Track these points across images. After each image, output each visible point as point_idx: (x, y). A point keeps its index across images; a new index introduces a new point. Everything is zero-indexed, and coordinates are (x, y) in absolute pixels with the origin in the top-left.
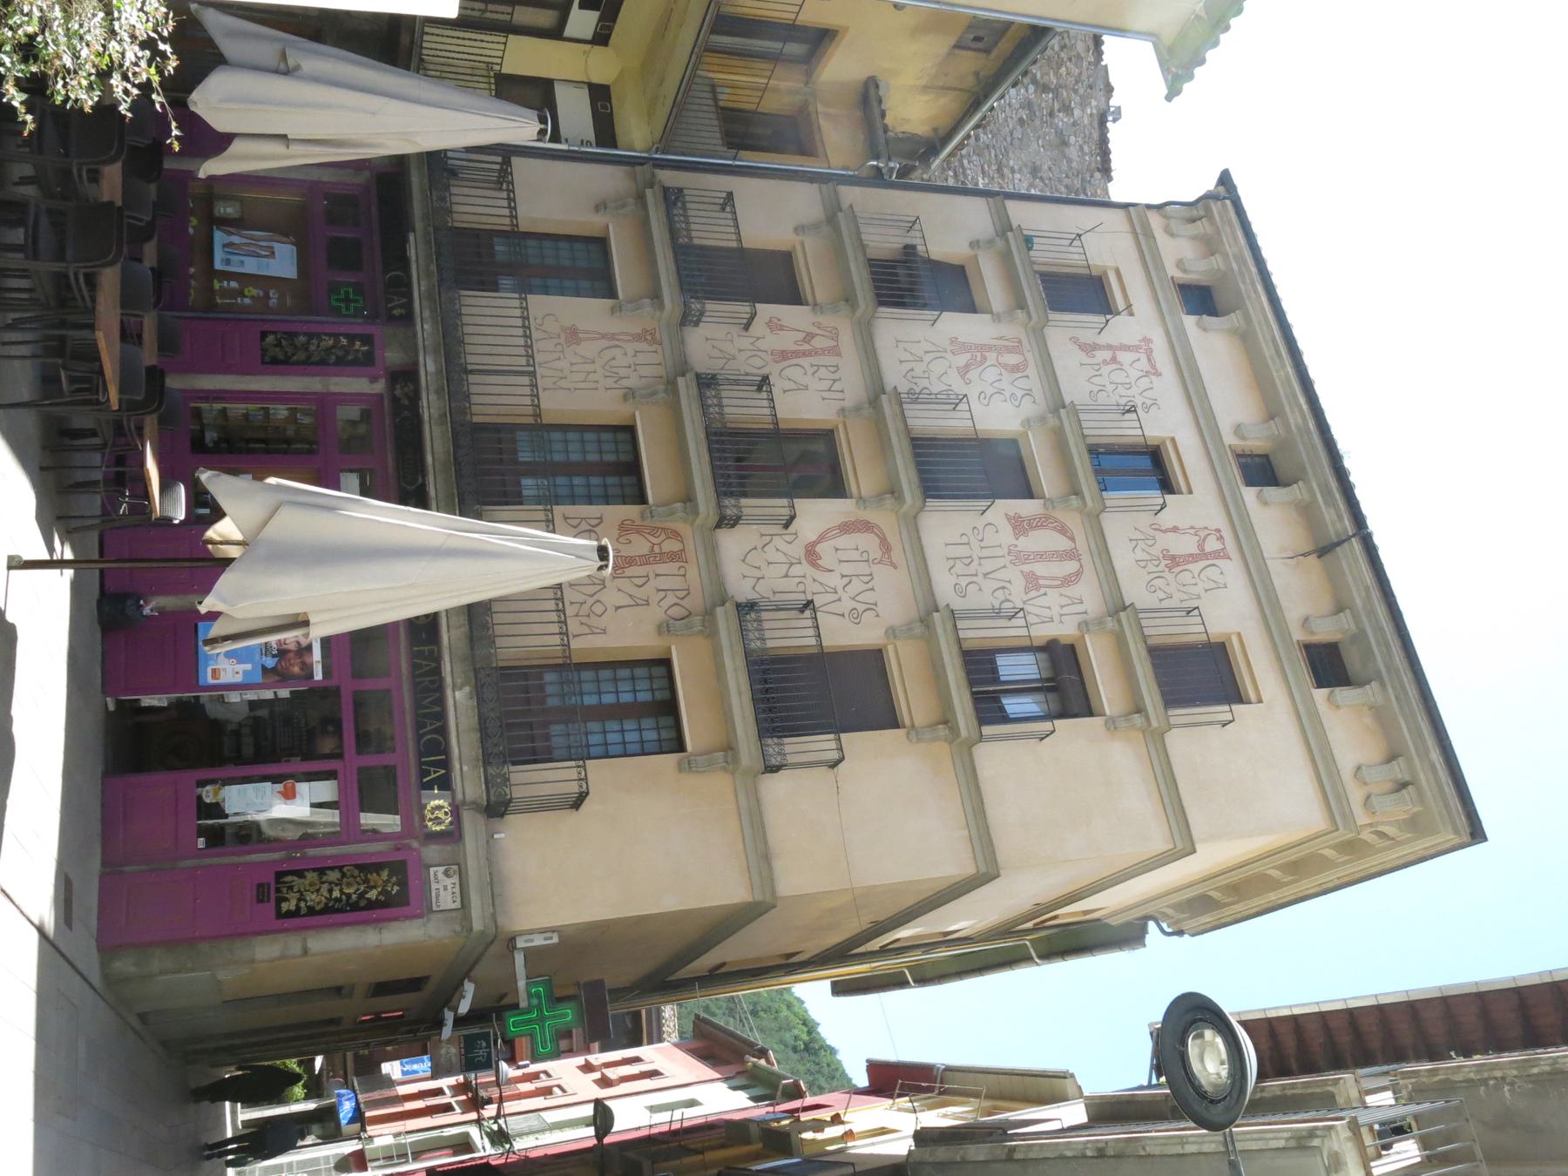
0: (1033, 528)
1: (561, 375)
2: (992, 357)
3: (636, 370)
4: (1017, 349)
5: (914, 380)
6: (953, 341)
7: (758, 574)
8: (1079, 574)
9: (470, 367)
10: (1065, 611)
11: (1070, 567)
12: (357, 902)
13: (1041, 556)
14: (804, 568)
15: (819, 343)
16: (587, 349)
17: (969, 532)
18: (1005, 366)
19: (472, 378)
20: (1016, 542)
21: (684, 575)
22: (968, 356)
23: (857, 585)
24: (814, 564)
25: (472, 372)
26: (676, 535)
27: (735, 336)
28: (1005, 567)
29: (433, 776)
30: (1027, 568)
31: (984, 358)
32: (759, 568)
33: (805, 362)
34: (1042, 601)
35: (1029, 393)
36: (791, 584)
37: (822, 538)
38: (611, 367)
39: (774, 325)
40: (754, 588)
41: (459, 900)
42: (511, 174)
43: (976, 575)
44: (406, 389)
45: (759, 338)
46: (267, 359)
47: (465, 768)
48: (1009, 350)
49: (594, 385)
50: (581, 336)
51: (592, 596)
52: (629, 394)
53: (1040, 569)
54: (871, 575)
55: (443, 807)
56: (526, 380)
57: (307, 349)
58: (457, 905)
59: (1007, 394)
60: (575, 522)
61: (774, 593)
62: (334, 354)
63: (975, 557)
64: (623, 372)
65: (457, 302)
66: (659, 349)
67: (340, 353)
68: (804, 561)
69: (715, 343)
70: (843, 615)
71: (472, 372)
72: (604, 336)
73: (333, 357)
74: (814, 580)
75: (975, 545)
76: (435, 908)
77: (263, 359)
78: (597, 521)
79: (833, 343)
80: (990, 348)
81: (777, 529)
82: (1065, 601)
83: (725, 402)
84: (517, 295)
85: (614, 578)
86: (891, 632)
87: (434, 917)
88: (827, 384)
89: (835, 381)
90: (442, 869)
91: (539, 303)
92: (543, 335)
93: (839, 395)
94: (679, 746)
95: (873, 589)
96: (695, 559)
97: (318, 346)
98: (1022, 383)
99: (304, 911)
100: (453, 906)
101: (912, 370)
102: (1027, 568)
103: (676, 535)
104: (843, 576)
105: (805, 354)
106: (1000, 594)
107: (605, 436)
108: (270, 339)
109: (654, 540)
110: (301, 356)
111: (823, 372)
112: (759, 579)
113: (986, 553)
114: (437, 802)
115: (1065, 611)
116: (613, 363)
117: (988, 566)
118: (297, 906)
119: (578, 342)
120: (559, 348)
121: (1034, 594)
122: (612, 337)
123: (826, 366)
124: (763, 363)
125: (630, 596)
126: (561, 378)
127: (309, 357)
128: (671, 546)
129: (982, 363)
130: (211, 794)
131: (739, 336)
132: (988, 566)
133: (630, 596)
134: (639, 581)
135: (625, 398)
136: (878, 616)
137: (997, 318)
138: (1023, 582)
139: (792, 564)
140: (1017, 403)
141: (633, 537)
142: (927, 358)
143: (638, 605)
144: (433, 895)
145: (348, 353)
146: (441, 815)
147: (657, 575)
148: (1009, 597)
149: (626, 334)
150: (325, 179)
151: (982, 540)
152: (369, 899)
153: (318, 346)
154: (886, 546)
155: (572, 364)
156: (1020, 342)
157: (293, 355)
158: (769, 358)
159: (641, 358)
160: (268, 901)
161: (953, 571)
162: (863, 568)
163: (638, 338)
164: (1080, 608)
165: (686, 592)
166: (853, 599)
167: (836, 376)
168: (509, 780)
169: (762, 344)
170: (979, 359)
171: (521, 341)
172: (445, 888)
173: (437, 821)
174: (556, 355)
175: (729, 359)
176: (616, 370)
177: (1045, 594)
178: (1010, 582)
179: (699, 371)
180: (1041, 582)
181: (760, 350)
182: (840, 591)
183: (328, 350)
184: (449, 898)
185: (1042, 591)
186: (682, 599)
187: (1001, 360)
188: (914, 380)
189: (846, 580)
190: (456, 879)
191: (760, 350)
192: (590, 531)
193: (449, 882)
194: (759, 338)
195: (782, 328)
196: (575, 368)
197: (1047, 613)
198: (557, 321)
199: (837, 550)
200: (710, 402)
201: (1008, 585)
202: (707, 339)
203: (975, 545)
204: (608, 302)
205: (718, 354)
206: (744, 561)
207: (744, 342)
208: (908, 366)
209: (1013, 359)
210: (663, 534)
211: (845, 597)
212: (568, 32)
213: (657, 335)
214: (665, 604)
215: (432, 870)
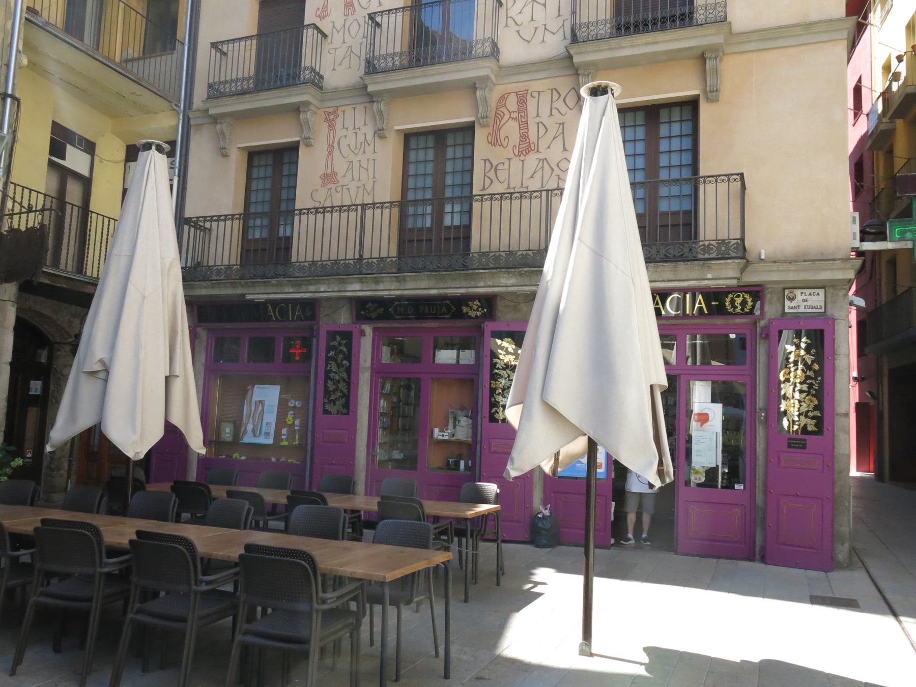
1: (361, 190)
3: (359, 128)
7: (541, 30)
9: (357, 256)
12: (815, 371)
16: (340, 167)
19: (366, 255)
21: (539, 93)
25: (361, 255)
26: (503, 98)
29: (703, 305)
32: (536, 29)
38: (356, 148)
39: (324, 12)
40: (554, 34)
41: (816, 291)
42: (198, 218)
44: (371, 309)
45: (334, 26)
46: (345, 411)
47: (709, 276)
49: (371, 162)
50: (329, 171)
51: (553, 170)
52: (380, 133)
56: (369, 213)
57: (338, 381)
58: (822, 292)
60: (488, 182)
62: (342, 361)
64: (361, 138)
65: (302, 264)
66: (340, 109)
67: (341, 356)
69: (338, 61)
71: (361, 255)
72: (330, 153)
73: (344, 362)
76: (823, 310)
77: (345, 414)
78: (488, 164)
81: (503, 11)
83: (390, 51)
84: (297, 218)
85: (538, 151)
87: (829, 312)
90: (787, 303)
91: (302, 200)
92: (329, 199)
94: (692, 105)
96: (525, 83)
97: (336, 373)
99: (817, 413)
100: (822, 297)
103: (503, 98)
107: (412, 156)
108: (329, 407)
109: (507, 117)
110: (342, 386)
112: (546, 29)
116: (353, 147)
118: (813, 418)
119: (334, 174)
120: (339, 189)
122: (331, 147)
124: (355, 24)
125: (555, 138)
126: (364, 188)
127: (344, 380)
128: (512, 103)
130: (698, 476)
133: (555, 138)
134: (542, 130)
135: (382, 137)
141: (503, 134)
143: (563, 132)
144: (810, 310)
145: (341, 351)
146: (739, 301)
147: (538, 116)
150: (203, 361)
152: (813, 362)
153: (336, 373)
155: (353, 179)
157: (341, 391)
158: (351, 18)
159: (349, 123)
160: (805, 440)
163: (332, 126)
168: (723, 241)
169: (339, 25)
171: (336, 215)
172: (804, 301)
174: (345, 191)
175: (351, 51)
176: (358, 146)
179: (364, 73)
181: (344, 25)
183: (339, 366)
184: (814, 298)
186: (560, 95)
190: (798, 292)
191: (344, 25)
192: (496, 170)
193: (800, 298)
194: (334, 26)
196: (356, 177)
198: (317, 190)
200: (390, 64)
202: (334, 69)
204: (302, 151)
206: (529, 42)
207: (337, 38)
210: (501, 109)
212: (85, 172)
213: (330, 110)
214: (563, 109)
215: (787, 310)
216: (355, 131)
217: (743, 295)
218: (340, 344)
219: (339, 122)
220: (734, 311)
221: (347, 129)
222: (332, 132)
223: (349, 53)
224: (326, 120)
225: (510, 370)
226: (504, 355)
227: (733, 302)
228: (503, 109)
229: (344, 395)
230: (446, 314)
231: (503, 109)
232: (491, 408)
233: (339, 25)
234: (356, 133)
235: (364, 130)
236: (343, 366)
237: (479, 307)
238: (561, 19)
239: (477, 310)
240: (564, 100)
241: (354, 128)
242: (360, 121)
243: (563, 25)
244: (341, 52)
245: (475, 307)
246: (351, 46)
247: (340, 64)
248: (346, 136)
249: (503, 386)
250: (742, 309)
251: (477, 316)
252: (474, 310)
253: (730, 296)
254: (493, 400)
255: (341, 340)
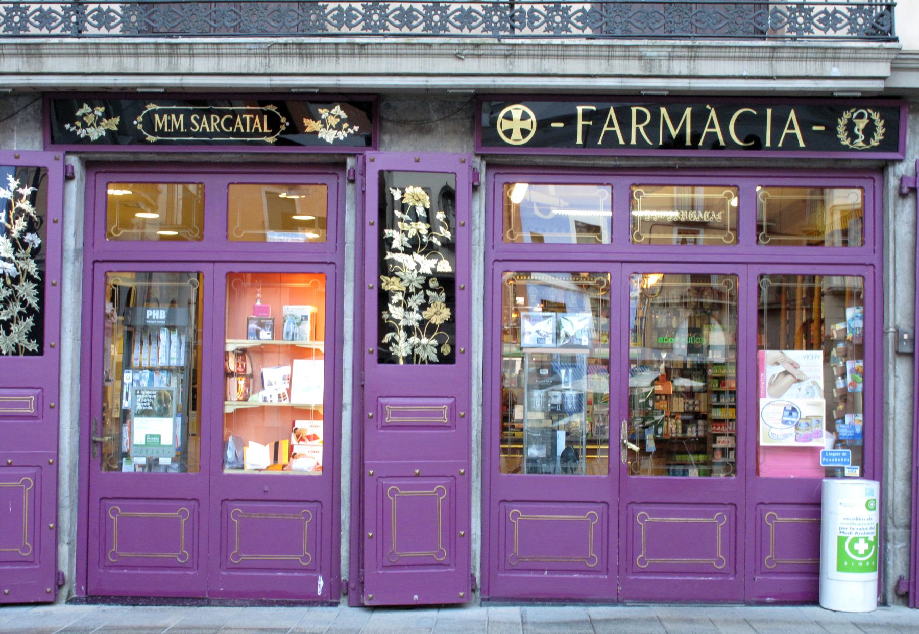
29: (797, 131)
44: (90, 120)
46: (33, 346)
47: (835, 72)
55: (850, 120)
57: (16, 280)
62: (23, 233)
73: (29, 237)
77: (33, 353)
110: (27, 290)
114: (841, 129)
127: (30, 278)
145: (20, 211)
146: (861, 124)
157: (24, 302)
173: (869, 130)
217: (869, 115)
218: (18, 196)
220: (851, 143)
225: (421, 254)
226: (408, 222)
227: (850, 125)
229: (31, 310)
230: (268, 135)
232: (381, 335)
236: (25, 246)
237: (342, 121)
239: (339, 127)
245: (333, 121)
249: (408, 288)
250: (867, 141)
251: (336, 140)
252: (331, 127)
253: (846, 115)
254: (385, 315)
255: (21, 186)
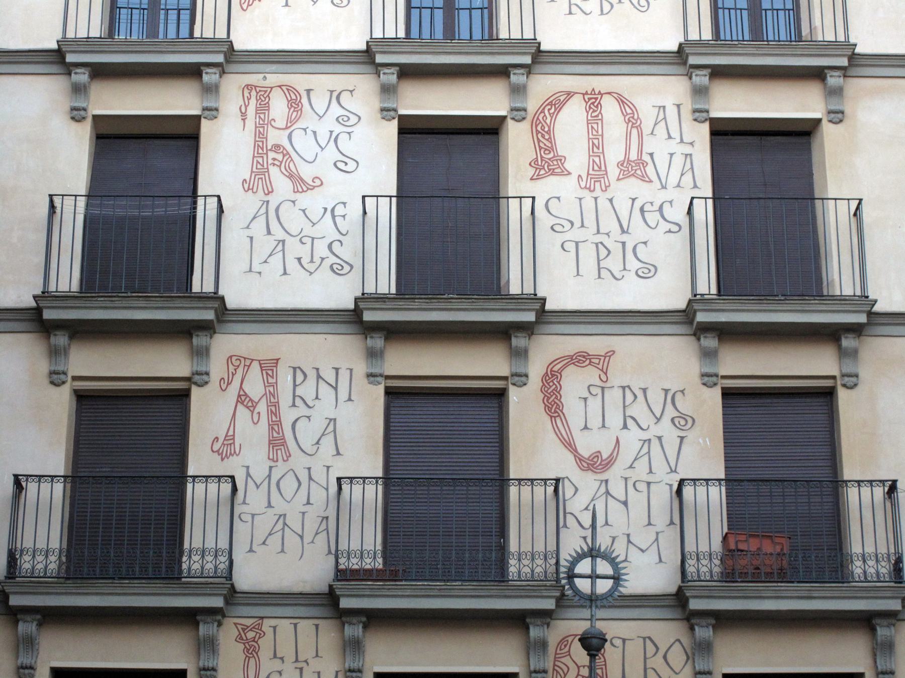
0: (551, 149)
2: (275, 137)
3: (306, 661)
4: (263, 97)
5: (317, 260)
6: (248, 187)
8: (622, 101)
10: (675, 134)
11: (610, 108)
13: (596, 146)
14: (615, 474)
15: (255, 386)
17: (559, 238)
18: (290, 123)
20: (574, 177)
21: (624, 640)
22: (274, 170)
23: (638, 410)
24: (609, 463)
27: (244, 508)
28: (611, 200)
30: (613, 172)
31: (277, 148)
33: (288, 416)
34: (662, 162)
35: (336, 96)
36: (637, 500)
37: (570, 445)
43: (624, 244)
48: (264, 107)
53: (614, 154)
54: (623, 388)
59: (338, 129)
61: (650, 524)
63: (598, 239)
66: (267, 623)
68: (604, 476)
70: (682, 438)
74: (631, 467)
75: (577, 234)
79: (255, 365)
80: (260, 137)
82: (661, 129)
86: (708, 379)
88: (324, 389)
89: (319, 377)
93: (344, 376)
95: (644, 390)
98: (320, 103)
101: (299, 259)
102: (613, 172)
104: (625, 426)
105: (274, 410)
106: (653, 218)
111: (307, 390)
112: (629, 541)
113: (590, 221)
115: (675, 134)
117: (609, 224)
121: (650, 170)
123: (295, 386)
124: (290, 477)
129: (286, 154)
131: (244, 503)
132: (609, 224)
136: (682, 392)
137: (212, 112)
138: (633, 180)
139: (607, 492)
140: (353, 119)
142: (279, 233)
148: (656, 207)
149: (246, 668)
151: (572, 224)
154: (580, 359)
156: (249, 87)
159: (286, 649)
161: (618, 276)
162: (614, 396)
163: (251, 650)
164: (671, 112)
165: (648, 641)
166: (658, 420)
167: (312, 375)
169: (259, 472)
170: (280, 157)
175: (285, 524)
177: (651, 155)
178: (634, 200)
180: (633, 156)
181: (269, 476)
182: (645, 436)
185: (646, 158)
186: (657, 649)
187: (281, 123)
188: (317, 260)
189: (630, 422)
191: (269, 476)
195: (230, 439)
197: (678, 160)
199: (586, 428)
201: (638, 204)
202: (251, 550)
203: (577, 234)
205: (275, 540)
208: (292, 265)
209: (279, 106)
210: (563, 660)
211: (655, 431)
216: (300, 665)
219: (265, 644)
221: (282, 659)
222: (252, 661)
223: (280, 525)
224: (239, 639)
228: (567, 660)
231: (567, 660)
233: (259, 472)
234: (301, 669)
235: (315, 665)
238: (652, 531)
240: (665, 657)
241: (297, 661)
242: (307, 652)
243: (657, 539)
244: (265, 523)
246: (285, 515)
247: (264, 543)
248: (280, 673)
